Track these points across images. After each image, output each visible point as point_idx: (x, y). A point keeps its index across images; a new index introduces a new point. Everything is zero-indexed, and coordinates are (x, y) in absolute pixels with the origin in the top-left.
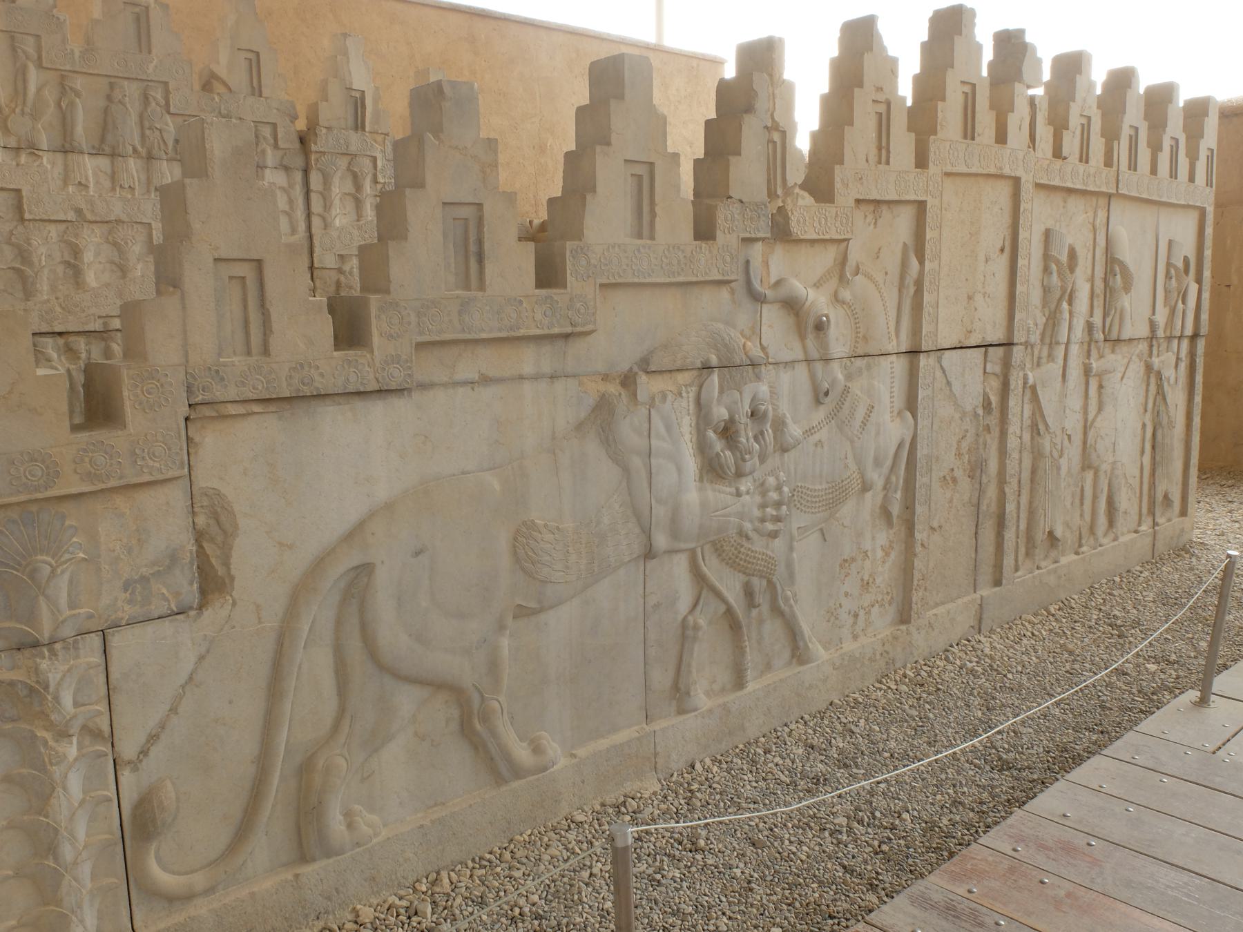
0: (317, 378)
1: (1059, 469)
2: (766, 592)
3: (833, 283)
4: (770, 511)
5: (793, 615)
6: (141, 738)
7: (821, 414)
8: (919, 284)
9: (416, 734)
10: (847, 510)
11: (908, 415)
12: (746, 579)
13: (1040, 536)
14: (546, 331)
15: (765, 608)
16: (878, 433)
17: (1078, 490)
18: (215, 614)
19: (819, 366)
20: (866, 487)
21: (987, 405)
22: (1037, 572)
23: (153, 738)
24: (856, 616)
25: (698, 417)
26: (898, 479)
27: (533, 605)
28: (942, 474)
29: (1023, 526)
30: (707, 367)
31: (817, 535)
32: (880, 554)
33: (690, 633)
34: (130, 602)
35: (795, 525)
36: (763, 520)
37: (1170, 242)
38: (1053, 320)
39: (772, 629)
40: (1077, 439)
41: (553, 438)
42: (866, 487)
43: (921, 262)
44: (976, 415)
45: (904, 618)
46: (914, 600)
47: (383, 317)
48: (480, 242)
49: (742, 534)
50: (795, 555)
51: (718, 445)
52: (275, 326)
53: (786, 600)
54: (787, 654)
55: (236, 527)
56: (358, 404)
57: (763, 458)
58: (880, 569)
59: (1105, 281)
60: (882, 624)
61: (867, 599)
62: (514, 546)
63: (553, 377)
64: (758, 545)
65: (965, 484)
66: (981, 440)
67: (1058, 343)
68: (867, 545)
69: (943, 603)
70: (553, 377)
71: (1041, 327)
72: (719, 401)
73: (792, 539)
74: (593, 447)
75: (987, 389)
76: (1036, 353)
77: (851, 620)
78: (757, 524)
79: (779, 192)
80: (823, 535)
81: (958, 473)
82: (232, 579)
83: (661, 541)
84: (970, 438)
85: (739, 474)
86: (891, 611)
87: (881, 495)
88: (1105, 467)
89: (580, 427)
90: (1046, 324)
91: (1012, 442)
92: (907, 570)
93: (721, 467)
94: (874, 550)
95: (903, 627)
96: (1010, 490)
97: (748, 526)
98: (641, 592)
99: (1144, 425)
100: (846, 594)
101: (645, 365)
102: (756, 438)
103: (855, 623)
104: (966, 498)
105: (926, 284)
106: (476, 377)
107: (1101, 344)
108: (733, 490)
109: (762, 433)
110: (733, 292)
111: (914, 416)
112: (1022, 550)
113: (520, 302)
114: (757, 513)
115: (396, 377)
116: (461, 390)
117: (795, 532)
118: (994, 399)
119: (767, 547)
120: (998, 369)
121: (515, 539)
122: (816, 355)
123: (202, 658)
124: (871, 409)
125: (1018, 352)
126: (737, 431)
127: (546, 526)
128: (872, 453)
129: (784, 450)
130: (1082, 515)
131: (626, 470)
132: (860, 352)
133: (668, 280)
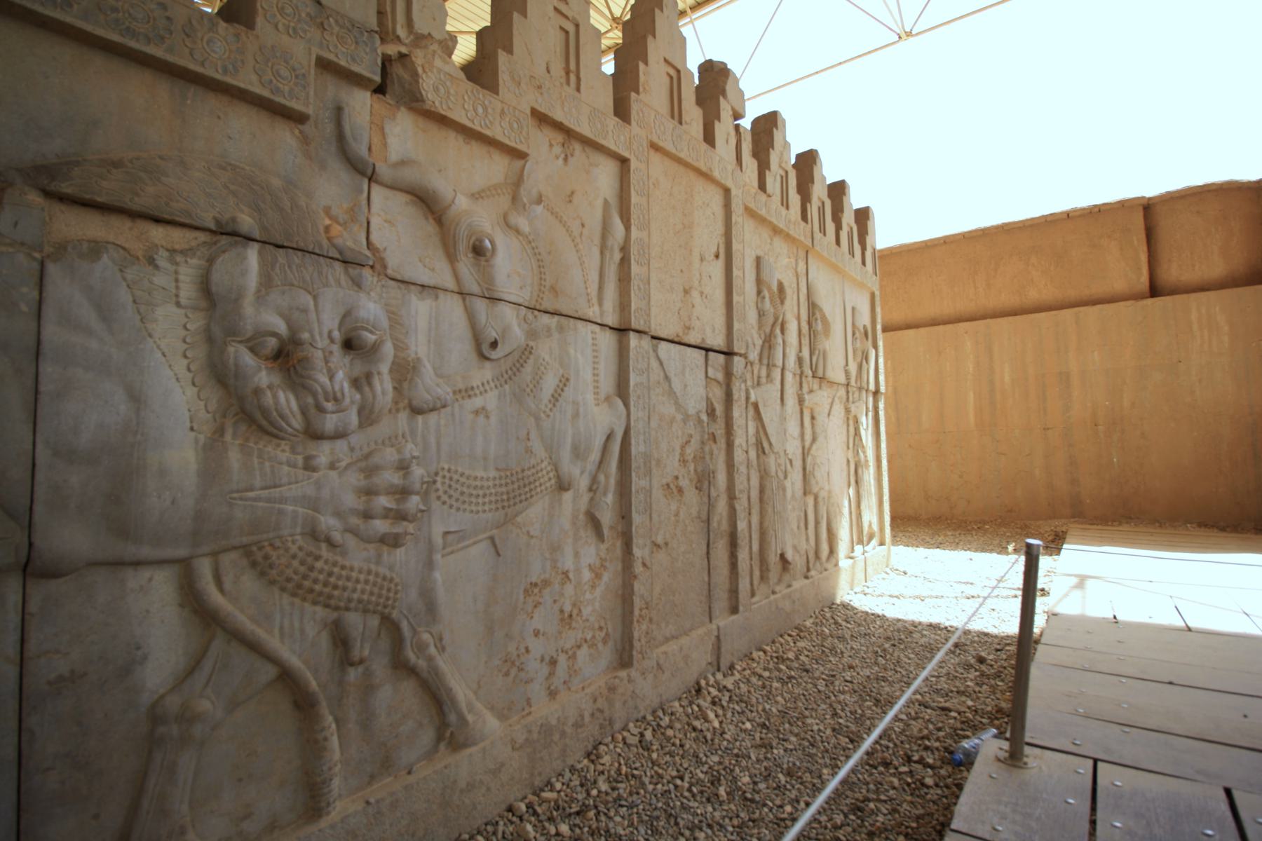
1: (784, 490)
3: (504, 201)
4: (384, 501)
5: (435, 671)
7: (485, 373)
8: (625, 249)
10: (535, 512)
11: (619, 403)
12: (335, 615)
13: (773, 559)
15: (380, 667)
16: (576, 415)
17: (802, 515)
19: (480, 306)
20: (562, 486)
21: (711, 413)
22: (772, 597)
24: (553, 662)
26: (607, 477)
28: (664, 481)
29: (756, 547)
30: (228, 233)
31: (484, 546)
32: (587, 575)
35: (437, 530)
36: (367, 516)
37: (853, 309)
38: (768, 343)
39: (395, 701)
40: (798, 463)
42: (562, 486)
43: (628, 228)
44: (700, 421)
45: (624, 659)
46: (636, 635)
49: (314, 534)
50: (437, 575)
53: (421, 648)
57: (368, 417)
58: (588, 596)
59: (809, 323)
60: (593, 666)
65: (691, 496)
66: (707, 449)
67: (774, 366)
68: (568, 563)
69: (674, 637)
71: (758, 348)
73: (431, 549)
75: (711, 395)
76: (756, 372)
77: (545, 670)
78: (354, 521)
79: (401, 32)
80: (495, 546)
81: (684, 483)
84: (695, 443)
86: (607, 654)
87: (586, 498)
88: (823, 494)
90: (762, 347)
91: (739, 456)
92: (626, 596)
93: (265, 412)
94: (578, 571)
95: (623, 674)
96: (741, 506)
97: (328, 522)
99: (848, 461)
100: (537, 633)
103: (551, 674)
104: (694, 511)
105: (634, 250)
107: (810, 379)
108: (300, 460)
109: (368, 376)
111: (626, 405)
112: (757, 573)
114: (350, 500)
117: (438, 540)
118: (719, 409)
120: (720, 376)
122: (475, 289)
124: (564, 382)
125: (738, 362)
126: (305, 360)
128: (569, 440)
129: (416, 411)
130: (807, 540)
133: (115, 37)
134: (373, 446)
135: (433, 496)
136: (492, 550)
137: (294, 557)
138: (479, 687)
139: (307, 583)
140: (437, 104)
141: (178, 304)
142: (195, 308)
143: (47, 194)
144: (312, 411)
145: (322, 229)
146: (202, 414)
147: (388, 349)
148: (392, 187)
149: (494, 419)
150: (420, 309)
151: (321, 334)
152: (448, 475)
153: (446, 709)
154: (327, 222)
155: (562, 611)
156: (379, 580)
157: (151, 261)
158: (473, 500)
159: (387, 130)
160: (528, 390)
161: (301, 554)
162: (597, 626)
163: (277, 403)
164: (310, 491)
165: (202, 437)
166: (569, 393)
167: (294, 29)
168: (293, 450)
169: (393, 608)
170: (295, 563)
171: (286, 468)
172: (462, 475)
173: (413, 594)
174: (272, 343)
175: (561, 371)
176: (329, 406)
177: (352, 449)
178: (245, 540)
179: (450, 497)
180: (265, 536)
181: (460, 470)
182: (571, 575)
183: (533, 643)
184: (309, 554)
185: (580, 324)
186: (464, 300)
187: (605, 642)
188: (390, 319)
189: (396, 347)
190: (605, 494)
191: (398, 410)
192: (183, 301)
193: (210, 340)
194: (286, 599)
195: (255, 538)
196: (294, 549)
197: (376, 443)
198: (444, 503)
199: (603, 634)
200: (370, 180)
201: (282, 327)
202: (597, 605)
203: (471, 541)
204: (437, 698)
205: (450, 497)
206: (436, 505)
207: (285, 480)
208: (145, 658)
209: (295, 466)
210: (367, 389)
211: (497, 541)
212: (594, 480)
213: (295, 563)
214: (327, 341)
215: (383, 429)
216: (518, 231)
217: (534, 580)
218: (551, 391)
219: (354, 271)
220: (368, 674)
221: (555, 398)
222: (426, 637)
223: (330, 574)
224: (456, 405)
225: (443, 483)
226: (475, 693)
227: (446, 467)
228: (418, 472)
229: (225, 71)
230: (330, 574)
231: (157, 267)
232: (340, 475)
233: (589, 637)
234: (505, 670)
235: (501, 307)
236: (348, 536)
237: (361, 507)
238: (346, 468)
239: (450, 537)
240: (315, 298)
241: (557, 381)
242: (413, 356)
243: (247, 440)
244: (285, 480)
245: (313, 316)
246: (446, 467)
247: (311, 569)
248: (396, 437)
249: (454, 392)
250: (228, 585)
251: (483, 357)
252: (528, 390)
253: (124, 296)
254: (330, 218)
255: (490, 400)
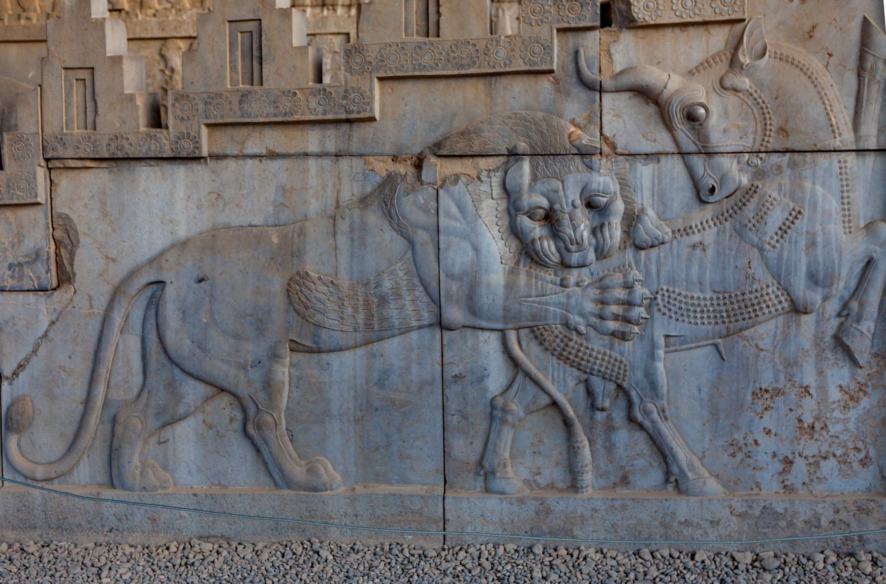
0: (127, 146)
2: (627, 402)
3: (722, 68)
4: (614, 309)
6: (15, 366)
7: (708, 212)
9: (204, 422)
10: (766, 331)
12: (585, 376)
14: (320, 117)
15: (619, 416)
16: (812, 244)
18: (61, 297)
19: (698, 162)
20: (797, 309)
23: (21, 366)
24: (788, 462)
25: (509, 202)
27: (308, 343)
30: (513, 155)
31: (709, 350)
32: (835, 395)
33: (498, 413)
34: (12, 277)
36: (602, 317)
41: (338, 207)
42: (797, 309)
47: (177, 105)
48: (260, 48)
49: (567, 325)
50: (660, 366)
51: (536, 230)
52: (100, 111)
53: (646, 413)
54: (656, 476)
55: (78, 241)
56: (167, 167)
58: (837, 414)
61: (811, 448)
62: (288, 290)
63: (338, 155)
64: (597, 344)
68: (810, 378)
70: (338, 155)
72: (531, 188)
73: (653, 346)
74: (374, 218)
77: (779, 467)
78: (593, 320)
82: (74, 274)
83: (455, 314)
85: (565, 265)
89: (364, 201)
94: (823, 388)
97: (575, 319)
98: (439, 360)
100: (768, 432)
101: (438, 150)
102: (594, 232)
106: (264, 152)
109: (602, 226)
110: (557, 81)
113: (295, 94)
114: (590, 307)
115: (187, 148)
116: (250, 162)
119: (612, 347)
121: (289, 285)
122: (692, 148)
123: (53, 323)
127: (319, 278)
129: (639, 248)
131: (411, 243)
132: (770, 147)
133: (456, 72)
134: (607, 272)
135: (655, 308)
136: (717, 356)
137: (557, 337)
138: (704, 456)
139: (565, 353)
140: (647, 18)
141: (492, 198)
142: (501, 198)
143: (440, 156)
144: (564, 250)
145: (566, 136)
146: (508, 255)
147: (619, 206)
148: (617, 91)
149: (710, 252)
150: (645, 172)
151: (567, 205)
152: (666, 294)
153: (669, 460)
154: (572, 129)
155: (800, 421)
156: (612, 361)
157: (479, 178)
158: (692, 315)
159: (612, 51)
160: (750, 225)
161: (560, 336)
162: (850, 445)
163: (542, 248)
164: (563, 300)
165: (507, 267)
166: (802, 224)
167: (542, 21)
168: (556, 274)
169: (624, 380)
170: (558, 340)
171: (550, 285)
172: (679, 294)
173: (639, 374)
174: (541, 212)
175: (792, 205)
176: (573, 248)
177: (592, 274)
178: (530, 324)
179: (670, 310)
180: (539, 323)
181: (677, 291)
182: (812, 391)
183: (761, 438)
184: (565, 337)
185: (821, 158)
186: (683, 158)
187: (863, 463)
188: (620, 184)
189: (625, 202)
190: (859, 320)
191: (625, 248)
192: (495, 196)
193: (510, 214)
194: (555, 360)
195: (535, 323)
196: (556, 332)
197: (609, 270)
198: (664, 314)
199: (861, 456)
200: (601, 92)
201: (545, 203)
202: (851, 426)
203: (693, 345)
204: (662, 452)
205: (670, 310)
206: (657, 315)
207: (549, 292)
208: (489, 375)
209: (555, 284)
210: (599, 235)
211: (722, 348)
212: (845, 306)
213: (558, 340)
214: (571, 208)
215: (615, 260)
216: (736, 90)
217: (764, 386)
218: (779, 223)
219: (587, 160)
220: (609, 418)
221: (783, 230)
222: (650, 406)
223: (579, 351)
224: (675, 242)
225: (663, 300)
226: (700, 460)
227: (665, 288)
228: (640, 291)
229: (505, 65)
230: (579, 351)
231: (482, 181)
232: (583, 290)
233: (838, 453)
234: (731, 451)
235: (718, 159)
236: (590, 329)
237: (597, 312)
238: (587, 287)
239: (672, 340)
240: (562, 182)
241: (786, 215)
242: (640, 206)
243: (531, 268)
244: (549, 292)
245: (561, 193)
246: (665, 288)
247: (567, 345)
248: (624, 266)
249: (673, 232)
250: (524, 347)
251: (702, 202)
252: (750, 225)
253: (468, 199)
254: (575, 126)
255: (709, 236)
